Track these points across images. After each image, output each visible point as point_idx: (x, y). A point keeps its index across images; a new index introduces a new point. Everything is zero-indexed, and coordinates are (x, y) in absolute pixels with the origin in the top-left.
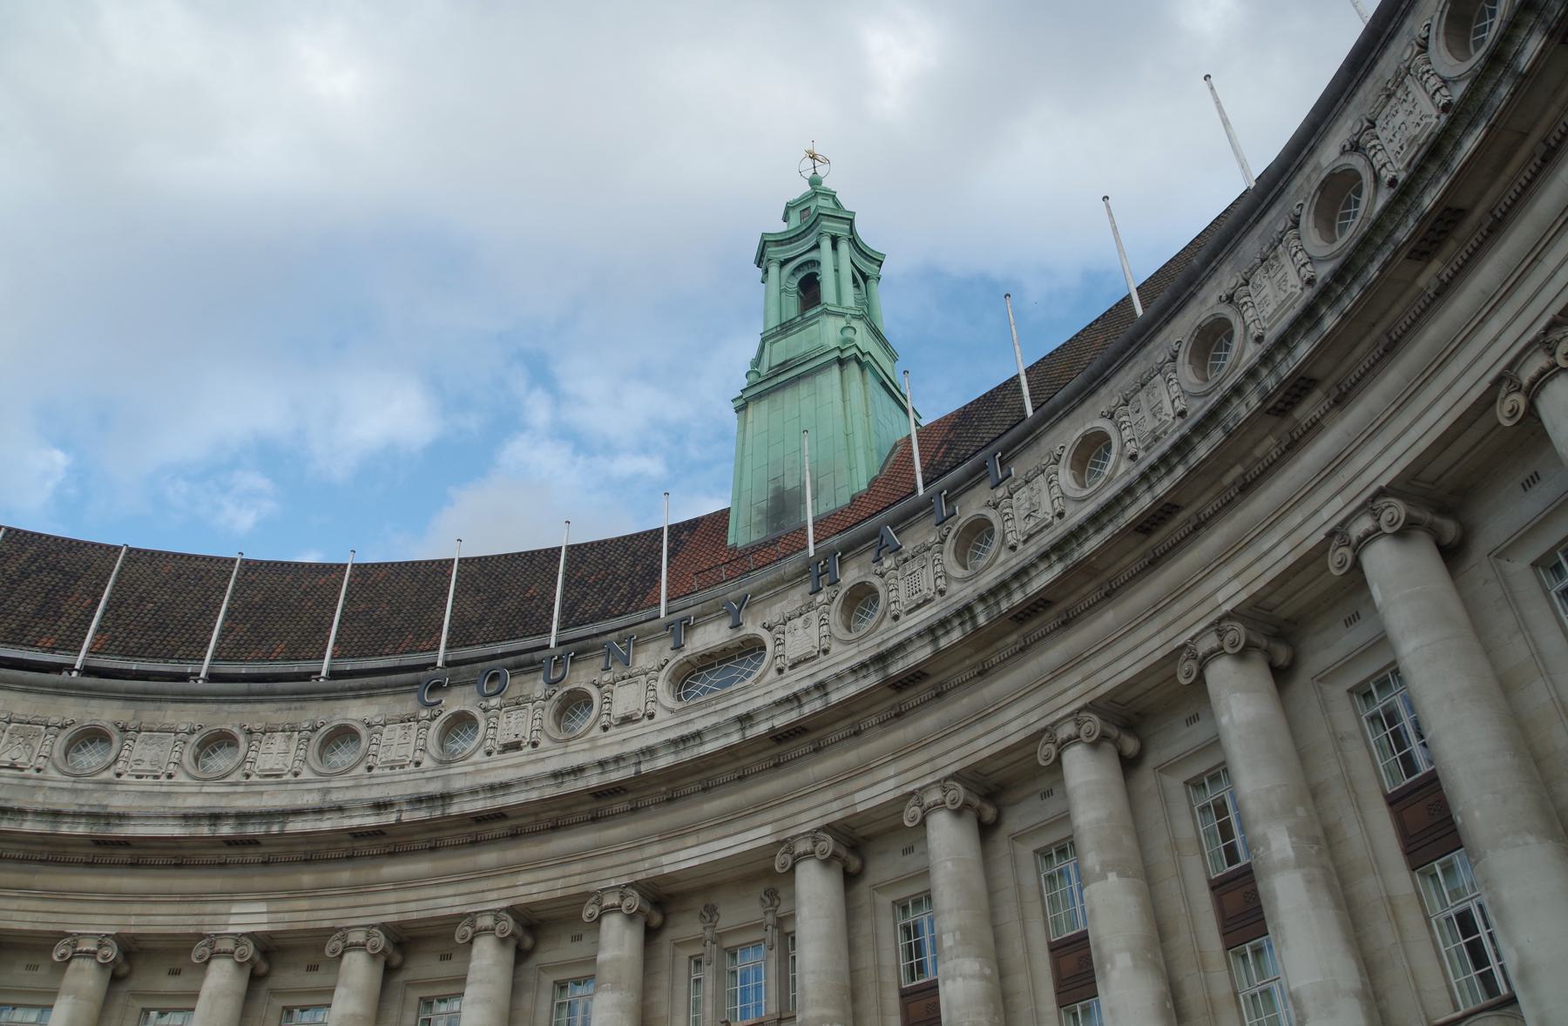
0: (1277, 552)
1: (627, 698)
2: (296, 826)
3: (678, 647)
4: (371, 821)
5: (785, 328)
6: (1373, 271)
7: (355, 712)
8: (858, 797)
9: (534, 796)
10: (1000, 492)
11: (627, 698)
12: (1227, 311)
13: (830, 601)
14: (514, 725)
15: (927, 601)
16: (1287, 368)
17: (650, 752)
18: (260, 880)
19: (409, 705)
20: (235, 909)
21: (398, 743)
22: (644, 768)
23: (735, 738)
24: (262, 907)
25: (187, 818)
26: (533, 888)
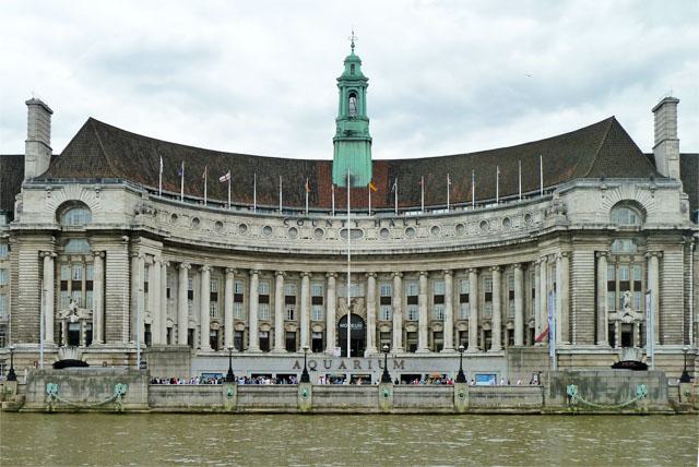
0: (459, 266)
7: (268, 222)
11: (331, 234)
13: (378, 229)
14: (306, 233)
19: (281, 223)
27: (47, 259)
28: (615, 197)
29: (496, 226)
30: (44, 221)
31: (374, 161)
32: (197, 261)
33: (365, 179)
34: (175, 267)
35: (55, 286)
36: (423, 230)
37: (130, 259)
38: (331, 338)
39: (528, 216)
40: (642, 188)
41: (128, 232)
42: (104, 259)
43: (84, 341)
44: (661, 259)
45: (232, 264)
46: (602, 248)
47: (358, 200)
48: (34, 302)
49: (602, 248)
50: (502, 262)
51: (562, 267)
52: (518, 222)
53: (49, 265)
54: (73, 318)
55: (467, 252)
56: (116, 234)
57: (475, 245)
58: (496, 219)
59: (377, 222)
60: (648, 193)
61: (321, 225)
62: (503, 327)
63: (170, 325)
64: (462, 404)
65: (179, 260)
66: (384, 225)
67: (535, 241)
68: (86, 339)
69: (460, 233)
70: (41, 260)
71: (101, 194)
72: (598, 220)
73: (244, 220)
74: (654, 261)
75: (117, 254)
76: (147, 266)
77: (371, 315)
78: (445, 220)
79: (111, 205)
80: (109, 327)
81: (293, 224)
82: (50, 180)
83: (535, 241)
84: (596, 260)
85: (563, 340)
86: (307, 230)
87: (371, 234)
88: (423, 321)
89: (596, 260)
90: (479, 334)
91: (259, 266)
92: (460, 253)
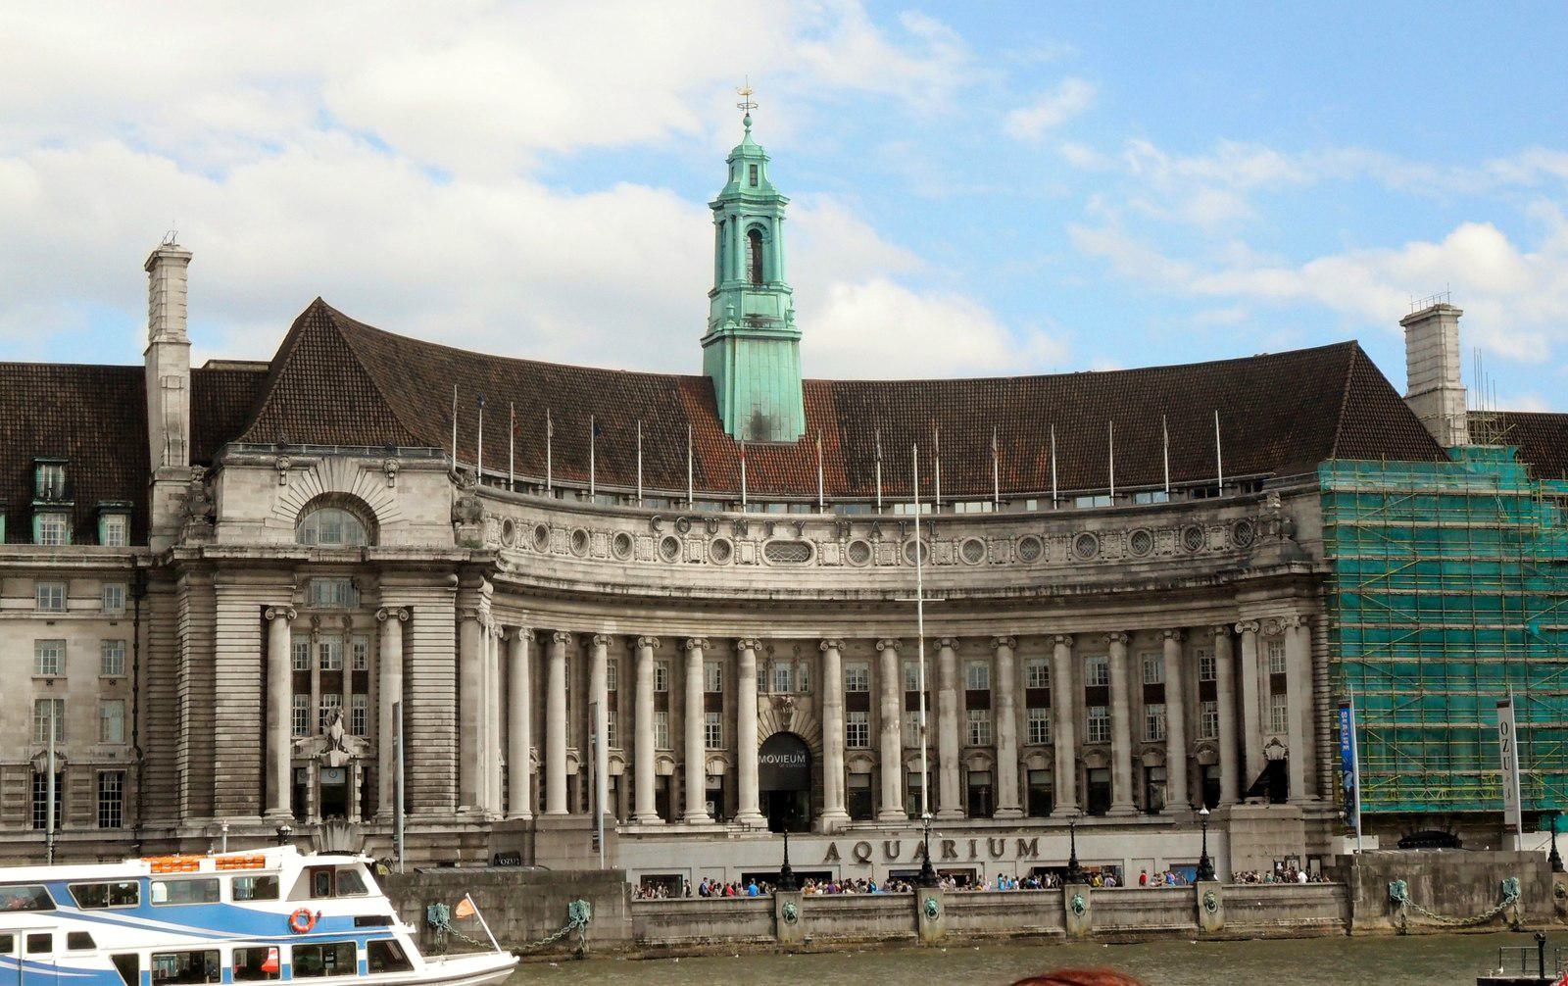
0: (1033, 628)
1: (748, 552)
2: (632, 591)
3: (771, 534)
4: (659, 593)
6: (1095, 591)
7: (626, 526)
8: (858, 632)
9: (725, 596)
10: (933, 540)
12: (1039, 540)
15: (891, 565)
16: (1061, 593)
17: (778, 592)
18: (613, 611)
19: (643, 527)
20: (605, 623)
21: (647, 546)
22: (774, 597)
23: (815, 598)
24: (614, 623)
25: (598, 584)
27: (281, 623)
29: (1114, 548)
30: (273, 538)
31: (804, 381)
33: (793, 426)
39: (1194, 532)
41: (460, 567)
42: (407, 626)
43: (358, 809)
45: (565, 623)
47: (777, 472)
48: (252, 722)
50: (1133, 624)
51: (1296, 651)
52: (1169, 545)
53: (283, 638)
54: (336, 758)
55: (1050, 602)
57: (1073, 587)
58: (1116, 533)
59: (841, 528)
61: (724, 533)
62: (1135, 762)
64: (1212, 921)
66: (857, 535)
67: (1225, 586)
68: (362, 803)
69: (1030, 558)
70: (266, 625)
71: (397, 482)
75: (434, 616)
78: (996, 530)
79: (414, 509)
80: (420, 775)
81: (667, 529)
82: (281, 446)
83: (1225, 586)
85: (1308, 792)
86: (697, 542)
87: (832, 553)
88: (950, 747)
90: (1077, 777)
91: (610, 627)
92: (1033, 604)
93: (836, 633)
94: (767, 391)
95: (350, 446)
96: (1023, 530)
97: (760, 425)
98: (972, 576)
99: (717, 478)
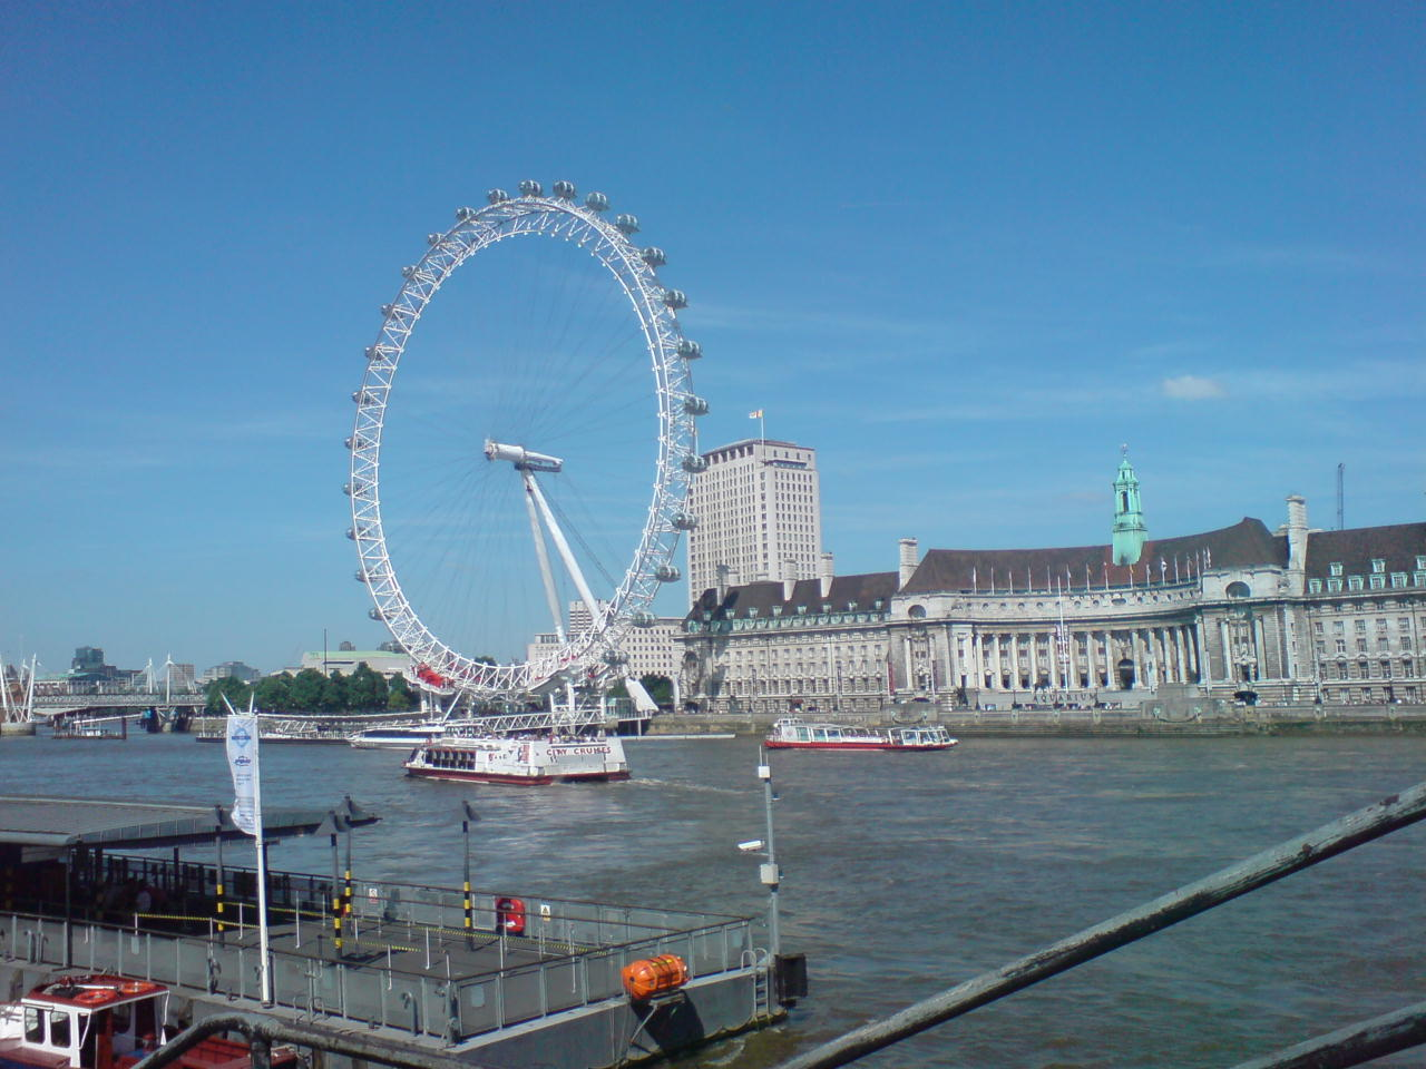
5: (1121, 514)
11: (1104, 603)
26: (1095, 629)
28: (1228, 580)
32: (1005, 632)
33: (1136, 557)
34: (988, 639)
35: (912, 655)
36: (1163, 597)
37: (949, 638)
38: (1111, 677)
40: (1247, 573)
41: (944, 623)
44: (1262, 620)
45: (1033, 631)
46: (1221, 616)
49: (1221, 616)
53: (907, 643)
56: (937, 624)
59: (1134, 593)
60: (1249, 576)
61: (1097, 598)
63: (988, 673)
65: (991, 632)
66: (1139, 594)
72: (1217, 598)
73: (1041, 600)
74: (1258, 623)
76: (960, 640)
77: (1136, 659)
79: (935, 607)
81: (1077, 598)
84: (1219, 625)
86: (1087, 602)
87: (1131, 599)
89: (1219, 625)
93: (1089, 630)
94: (1128, 547)
95: (919, 592)
96: (1180, 590)
97: (1123, 560)
98: (1168, 607)
99: (1097, 582)
